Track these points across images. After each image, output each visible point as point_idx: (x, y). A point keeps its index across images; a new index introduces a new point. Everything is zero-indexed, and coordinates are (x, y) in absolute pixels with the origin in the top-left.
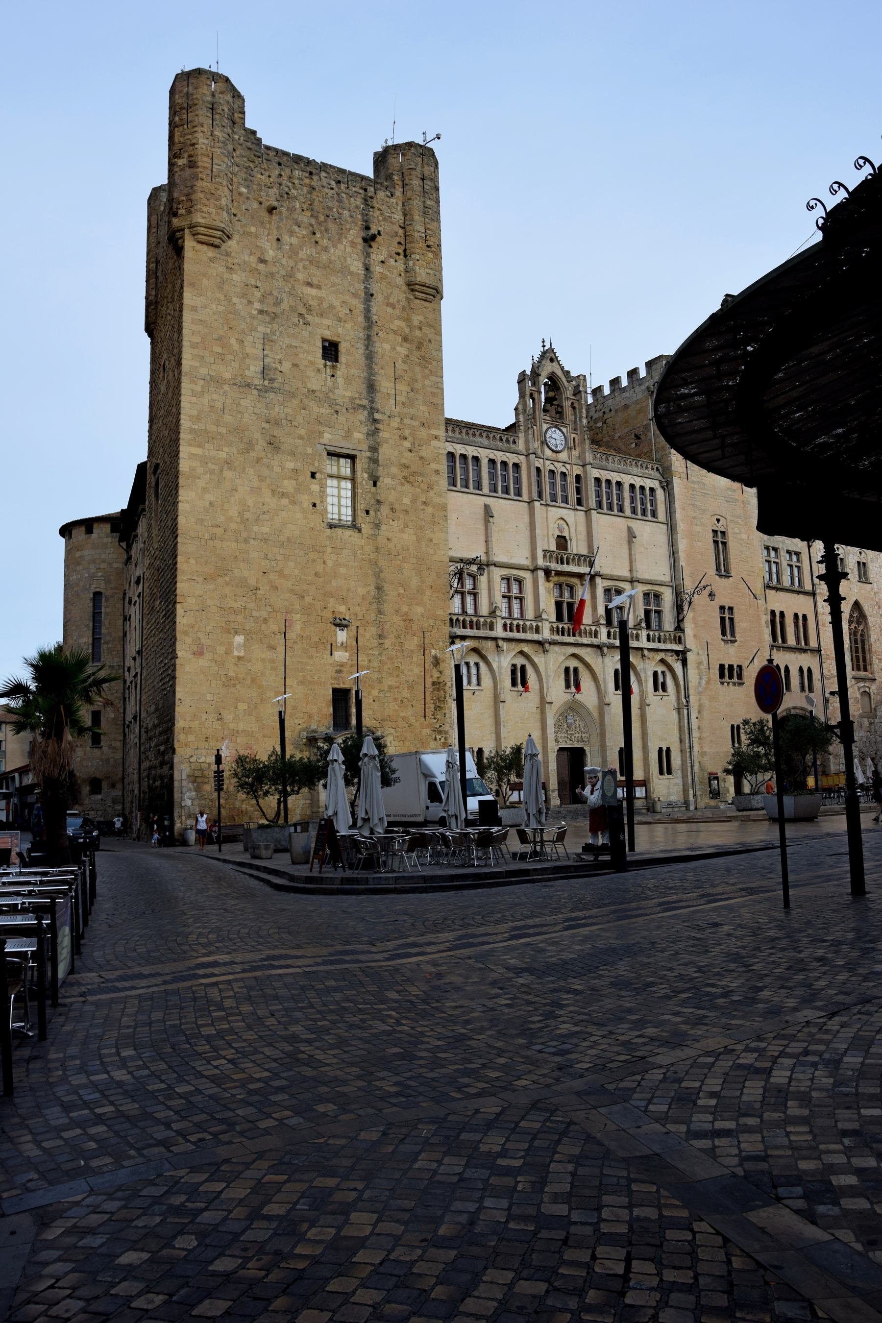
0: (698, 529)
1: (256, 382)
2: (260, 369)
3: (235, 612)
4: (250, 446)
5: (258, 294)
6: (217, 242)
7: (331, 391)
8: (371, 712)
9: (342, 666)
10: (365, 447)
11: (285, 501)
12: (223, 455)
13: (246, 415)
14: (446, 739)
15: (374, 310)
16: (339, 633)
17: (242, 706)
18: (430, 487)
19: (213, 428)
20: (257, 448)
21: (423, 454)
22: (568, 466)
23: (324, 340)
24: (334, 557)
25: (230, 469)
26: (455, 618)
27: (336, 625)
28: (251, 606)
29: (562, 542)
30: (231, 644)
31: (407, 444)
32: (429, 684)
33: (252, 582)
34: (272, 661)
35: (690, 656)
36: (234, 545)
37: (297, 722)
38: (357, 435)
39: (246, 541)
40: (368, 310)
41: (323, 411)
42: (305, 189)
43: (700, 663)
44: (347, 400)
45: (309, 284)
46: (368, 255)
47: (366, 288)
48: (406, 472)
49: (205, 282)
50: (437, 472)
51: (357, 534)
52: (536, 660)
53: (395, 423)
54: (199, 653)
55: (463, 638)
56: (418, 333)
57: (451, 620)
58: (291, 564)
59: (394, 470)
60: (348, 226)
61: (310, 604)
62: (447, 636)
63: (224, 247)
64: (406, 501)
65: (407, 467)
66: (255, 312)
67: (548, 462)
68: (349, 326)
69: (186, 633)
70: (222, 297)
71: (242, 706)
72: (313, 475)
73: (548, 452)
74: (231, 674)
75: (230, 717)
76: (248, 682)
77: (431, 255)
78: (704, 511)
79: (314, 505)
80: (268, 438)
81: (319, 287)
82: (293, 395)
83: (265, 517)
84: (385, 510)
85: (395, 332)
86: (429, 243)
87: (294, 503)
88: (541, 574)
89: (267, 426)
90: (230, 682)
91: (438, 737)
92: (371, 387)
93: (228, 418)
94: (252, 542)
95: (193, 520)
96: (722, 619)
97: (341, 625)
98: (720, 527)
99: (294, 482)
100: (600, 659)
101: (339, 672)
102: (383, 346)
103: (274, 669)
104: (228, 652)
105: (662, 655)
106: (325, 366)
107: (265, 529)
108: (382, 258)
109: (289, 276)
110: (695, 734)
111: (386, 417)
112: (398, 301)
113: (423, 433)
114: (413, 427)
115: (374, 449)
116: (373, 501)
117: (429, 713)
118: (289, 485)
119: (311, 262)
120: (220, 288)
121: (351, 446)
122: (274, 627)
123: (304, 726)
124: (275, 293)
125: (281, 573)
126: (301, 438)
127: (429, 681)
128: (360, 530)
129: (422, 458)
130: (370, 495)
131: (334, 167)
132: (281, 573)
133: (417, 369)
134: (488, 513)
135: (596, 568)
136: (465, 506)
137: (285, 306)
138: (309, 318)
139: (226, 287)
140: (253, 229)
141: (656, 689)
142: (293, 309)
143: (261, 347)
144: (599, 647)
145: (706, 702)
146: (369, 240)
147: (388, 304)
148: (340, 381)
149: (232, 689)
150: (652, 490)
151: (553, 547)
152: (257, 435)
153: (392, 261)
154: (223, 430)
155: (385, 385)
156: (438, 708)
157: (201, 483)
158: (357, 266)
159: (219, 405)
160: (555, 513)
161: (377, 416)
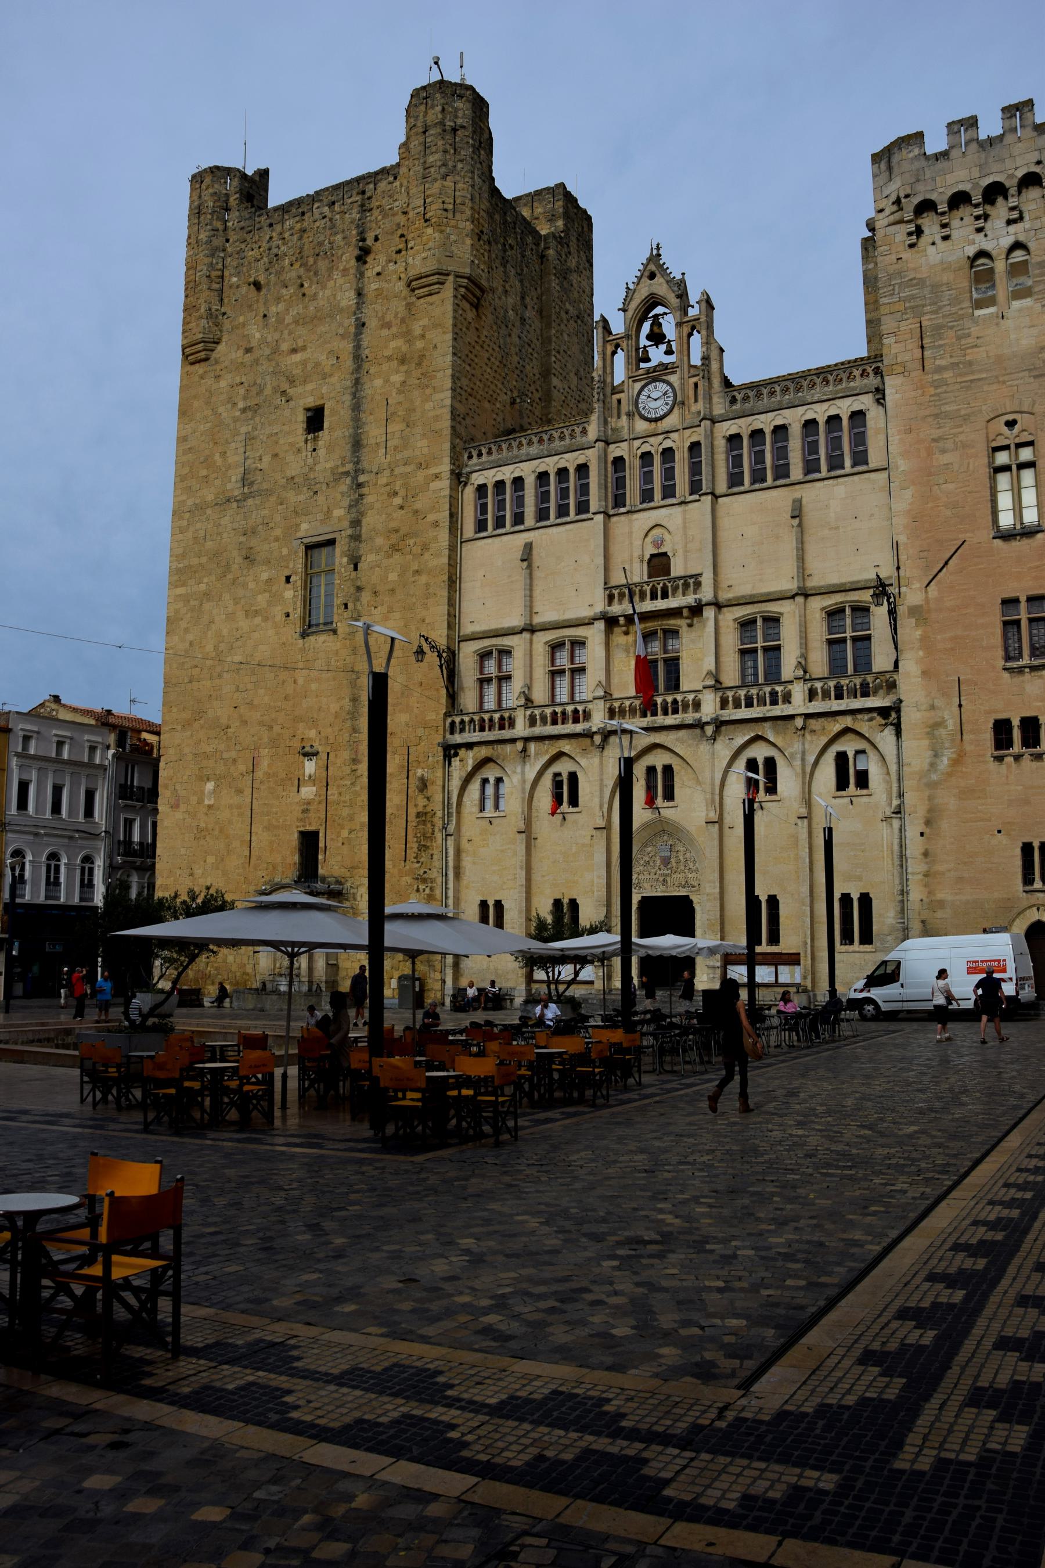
0: (946, 459)
1: (236, 493)
2: (240, 477)
3: (207, 756)
4: (228, 567)
5: (242, 391)
6: (202, 355)
7: (311, 469)
8: (339, 858)
9: (309, 803)
10: (346, 524)
11: (258, 620)
12: (203, 587)
13: (225, 535)
14: (432, 889)
15: (364, 344)
16: (307, 763)
17: (211, 859)
18: (425, 547)
19: (195, 561)
20: (235, 567)
21: (418, 505)
22: (674, 436)
23: (308, 410)
24: (305, 672)
25: (208, 600)
26: (457, 720)
27: (305, 755)
28: (222, 747)
29: (659, 563)
30: (202, 792)
31: (397, 501)
32: (412, 817)
33: (224, 721)
34: (239, 807)
35: (910, 716)
36: (208, 683)
37: (260, 873)
38: (338, 512)
39: (220, 676)
40: (358, 347)
41: (301, 498)
42: (295, 237)
43: (939, 724)
44: (328, 473)
45: (294, 351)
46: (362, 275)
47: (357, 319)
48: (394, 538)
49: (196, 404)
50: (436, 524)
51: (332, 637)
52: (583, 762)
53: (383, 480)
54: (175, 806)
55: (469, 746)
56: (419, 344)
57: (453, 723)
58: (262, 691)
59: (379, 541)
60: (340, 252)
61: (279, 735)
62: (440, 749)
63: (214, 355)
64: (393, 577)
65: (396, 531)
66: (238, 413)
67: (637, 443)
68: (334, 380)
69: (166, 787)
70: (210, 412)
71: (211, 859)
72: (288, 579)
73: (641, 426)
74: (202, 825)
75: (200, 871)
76: (216, 832)
77: (430, 231)
78: (966, 418)
79: (288, 615)
80: (244, 553)
81: (304, 348)
82: (269, 492)
83: (239, 643)
84: (366, 597)
85: (389, 358)
86: (427, 217)
87: (266, 619)
88: (600, 625)
89: (243, 539)
90: (201, 833)
91: (422, 887)
92: (357, 444)
93: (209, 544)
94: (225, 675)
95: (175, 666)
96: (1011, 625)
97: (309, 755)
98: (1009, 436)
99: (267, 595)
100: (705, 747)
101: (305, 811)
102: (374, 386)
103: (240, 815)
104: (200, 801)
105: (848, 721)
106: (306, 441)
107: (238, 658)
108: (378, 269)
109: (276, 351)
110: (916, 866)
111: (373, 475)
112: (396, 316)
113: (421, 475)
114: (405, 476)
115: (356, 523)
116: (352, 590)
117: (411, 854)
118: (262, 600)
119: (297, 322)
120: (208, 403)
121: (330, 529)
122: (242, 768)
123: (267, 878)
124: (259, 381)
125: (250, 704)
126: (277, 539)
127: (412, 811)
128: (334, 632)
129: (416, 512)
130: (349, 583)
131: (326, 189)
132: (250, 704)
133: (416, 393)
134: (527, 555)
135: (706, 594)
136: (491, 558)
137: (268, 391)
138: (291, 392)
139: (214, 399)
140: (241, 319)
141: (842, 784)
142: (275, 390)
143: (242, 450)
144: (700, 725)
145: (948, 800)
146: (363, 255)
147: (382, 327)
148: (322, 452)
149: (202, 842)
150: (858, 416)
151: (639, 574)
152: (235, 553)
153: (391, 267)
154: (204, 560)
155: (373, 432)
156: (423, 848)
157: (183, 624)
158: (347, 299)
159: (202, 533)
160: (644, 519)
161: (362, 479)
